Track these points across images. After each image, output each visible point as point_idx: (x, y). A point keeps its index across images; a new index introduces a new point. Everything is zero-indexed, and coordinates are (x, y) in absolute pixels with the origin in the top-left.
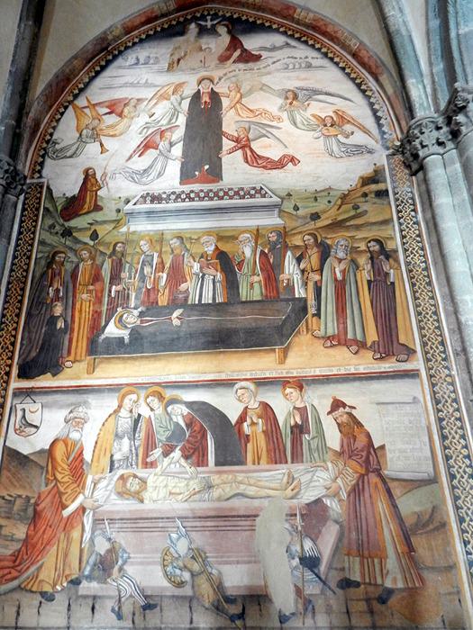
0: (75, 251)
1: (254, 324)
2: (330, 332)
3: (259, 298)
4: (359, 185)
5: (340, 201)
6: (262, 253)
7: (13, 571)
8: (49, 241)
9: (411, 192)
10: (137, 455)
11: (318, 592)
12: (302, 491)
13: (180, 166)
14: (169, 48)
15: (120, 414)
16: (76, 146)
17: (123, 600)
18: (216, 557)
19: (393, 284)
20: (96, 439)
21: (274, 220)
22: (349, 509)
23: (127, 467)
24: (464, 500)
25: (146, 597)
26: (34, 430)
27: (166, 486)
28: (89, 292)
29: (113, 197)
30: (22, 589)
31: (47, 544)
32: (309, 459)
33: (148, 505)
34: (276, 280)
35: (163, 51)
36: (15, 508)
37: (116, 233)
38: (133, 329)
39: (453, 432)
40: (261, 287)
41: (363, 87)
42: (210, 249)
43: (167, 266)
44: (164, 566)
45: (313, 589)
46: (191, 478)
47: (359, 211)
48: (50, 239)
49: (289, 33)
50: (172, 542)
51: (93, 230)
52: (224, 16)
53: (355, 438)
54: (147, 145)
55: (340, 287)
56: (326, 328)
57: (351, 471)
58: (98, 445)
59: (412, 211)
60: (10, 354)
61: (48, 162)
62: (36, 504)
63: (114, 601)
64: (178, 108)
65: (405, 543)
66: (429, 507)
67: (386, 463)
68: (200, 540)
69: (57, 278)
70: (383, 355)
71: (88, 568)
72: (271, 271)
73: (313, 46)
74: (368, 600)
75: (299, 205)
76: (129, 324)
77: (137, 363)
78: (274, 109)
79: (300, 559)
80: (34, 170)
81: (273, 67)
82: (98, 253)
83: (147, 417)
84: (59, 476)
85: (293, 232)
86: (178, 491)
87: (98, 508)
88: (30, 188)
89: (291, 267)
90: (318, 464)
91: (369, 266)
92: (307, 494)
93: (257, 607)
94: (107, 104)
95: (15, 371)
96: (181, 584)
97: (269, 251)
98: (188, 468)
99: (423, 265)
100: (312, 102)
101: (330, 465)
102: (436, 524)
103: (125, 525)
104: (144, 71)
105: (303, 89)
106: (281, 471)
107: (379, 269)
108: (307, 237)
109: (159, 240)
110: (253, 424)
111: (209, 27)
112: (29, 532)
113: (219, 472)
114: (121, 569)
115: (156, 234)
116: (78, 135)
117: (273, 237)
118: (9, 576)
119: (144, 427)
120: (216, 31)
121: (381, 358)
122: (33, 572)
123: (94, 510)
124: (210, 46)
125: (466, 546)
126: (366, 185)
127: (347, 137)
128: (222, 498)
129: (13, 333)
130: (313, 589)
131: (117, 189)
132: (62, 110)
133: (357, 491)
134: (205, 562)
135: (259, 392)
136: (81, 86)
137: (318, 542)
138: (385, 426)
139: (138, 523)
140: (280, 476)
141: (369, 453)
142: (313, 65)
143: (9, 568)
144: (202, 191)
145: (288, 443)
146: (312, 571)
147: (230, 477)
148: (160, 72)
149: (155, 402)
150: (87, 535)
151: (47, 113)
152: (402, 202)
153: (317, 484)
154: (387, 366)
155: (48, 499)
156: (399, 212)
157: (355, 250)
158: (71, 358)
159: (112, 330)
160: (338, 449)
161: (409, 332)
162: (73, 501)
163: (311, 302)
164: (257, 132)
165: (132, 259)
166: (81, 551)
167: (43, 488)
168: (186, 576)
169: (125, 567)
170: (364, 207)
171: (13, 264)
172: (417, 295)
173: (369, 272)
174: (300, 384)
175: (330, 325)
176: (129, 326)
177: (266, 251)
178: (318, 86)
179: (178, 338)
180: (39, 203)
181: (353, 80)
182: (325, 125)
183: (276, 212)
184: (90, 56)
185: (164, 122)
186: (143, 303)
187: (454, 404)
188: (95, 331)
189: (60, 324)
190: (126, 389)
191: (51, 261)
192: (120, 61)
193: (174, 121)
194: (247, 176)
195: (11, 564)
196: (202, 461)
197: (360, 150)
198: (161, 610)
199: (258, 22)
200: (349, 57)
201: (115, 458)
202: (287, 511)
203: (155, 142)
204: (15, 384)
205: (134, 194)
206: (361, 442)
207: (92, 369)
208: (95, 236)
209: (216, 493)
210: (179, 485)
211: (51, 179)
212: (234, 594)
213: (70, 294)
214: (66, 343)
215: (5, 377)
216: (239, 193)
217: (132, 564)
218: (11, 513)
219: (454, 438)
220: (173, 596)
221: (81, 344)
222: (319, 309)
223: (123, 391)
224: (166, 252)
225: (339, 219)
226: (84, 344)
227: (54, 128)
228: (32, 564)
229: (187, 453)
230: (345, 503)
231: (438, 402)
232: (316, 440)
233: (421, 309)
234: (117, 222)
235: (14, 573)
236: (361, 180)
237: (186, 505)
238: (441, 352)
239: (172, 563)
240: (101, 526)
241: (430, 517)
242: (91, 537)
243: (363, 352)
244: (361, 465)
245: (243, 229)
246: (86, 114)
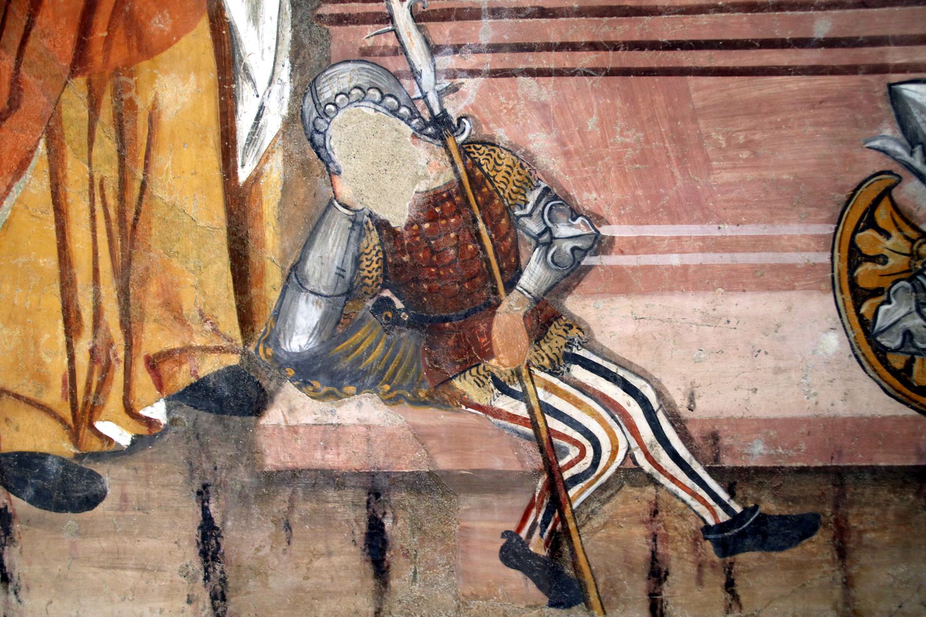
17: (577, 494)
25: (733, 479)
44: (859, 295)
63: (522, 502)
114: (544, 317)
150: (266, 98)
166: (238, 202)
169: (573, 305)
198: (842, 553)
217: (623, 283)
240: (368, 35)
242: (295, 118)
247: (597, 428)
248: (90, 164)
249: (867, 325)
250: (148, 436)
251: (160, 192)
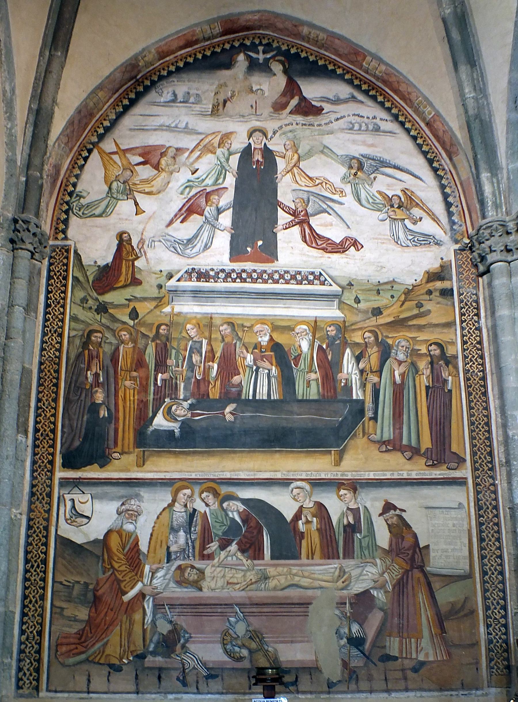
0: (113, 331)
1: (310, 425)
2: (386, 437)
3: (316, 397)
4: (424, 281)
5: (403, 296)
6: (320, 347)
7: (78, 646)
8: (81, 317)
9: (476, 294)
10: (194, 548)
11: (361, 664)
12: (352, 584)
13: (230, 238)
14: (213, 84)
15: (175, 509)
16: (105, 202)
17: (187, 671)
18: (273, 637)
19: (450, 391)
20: (151, 531)
21: (331, 312)
22: (393, 599)
23: (184, 558)
24: (492, 593)
26: (85, 520)
27: (224, 576)
28: (132, 379)
29: (153, 269)
30: (90, 662)
31: (110, 625)
32: (359, 556)
33: (206, 593)
34: (334, 380)
35: (206, 87)
36: (75, 592)
37: (158, 313)
38: (183, 422)
39: (490, 535)
40: (318, 385)
41: (435, 165)
42: (264, 340)
43: (218, 355)
44: (224, 644)
45: (357, 662)
46: (248, 570)
47: (422, 310)
49: (356, 82)
50: (230, 625)
51: (131, 307)
52: (279, 48)
53: (403, 538)
54: (190, 210)
55: (398, 391)
56: (382, 432)
57: (397, 567)
58: (154, 537)
59: (475, 315)
60: (51, 442)
61: (74, 220)
62: (95, 590)
64: (225, 164)
65: (439, 627)
66: (462, 597)
67: (429, 561)
68: (256, 623)
69: (95, 361)
70: (435, 462)
71: (152, 646)
73: (382, 104)
74: (403, 670)
75: (361, 297)
76: (179, 416)
77: (189, 458)
78: (336, 180)
79: (348, 639)
80: (57, 228)
81: (336, 125)
82: (140, 335)
83: (203, 512)
84: (116, 566)
85: (353, 327)
86: (235, 581)
87: (157, 594)
88: (55, 251)
89: (350, 366)
90: (368, 560)
91: (429, 371)
92: (356, 586)
93: (309, 677)
94: (140, 151)
95: (58, 460)
96: (241, 659)
97: (327, 346)
98: (244, 560)
99: (480, 374)
100: (380, 176)
101: (378, 561)
102: (466, 611)
103: (185, 610)
104: (183, 110)
105: (369, 158)
107: (438, 375)
108: (367, 335)
109: (207, 324)
110: (308, 522)
111: (261, 61)
112: (91, 614)
113: (276, 566)
115: (206, 318)
116: (106, 188)
117: (332, 331)
118: (76, 651)
119: (199, 522)
120: (269, 67)
121: (433, 466)
122: (99, 648)
123: (154, 596)
124: (262, 87)
125: (488, 628)
126: (431, 281)
127: (415, 223)
128: (278, 588)
129: (52, 419)
130: (357, 662)
131: (158, 260)
132: (85, 154)
134: (261, 641)
135: (314, 492)
136: (107, 123)
137: (364, 626)
138: (431, 528)
139: (200, 608)
140: (333, 570)
141: (414, 552)
142: (381, 128)
143: (74, 644)
144: (255, 271)
146: (358, 649)
147: (285, 570)
148: (203, 114)
149: (211, 499)
150: (149, 618)
151: (68, 156)
152: (467, 305)
153: (366, 577)
155: (107, 585)
156: (462, 315)
157: (414, 353)
158: (119, 449)
159: (160, 421)
160: (387, 548)
161: (461, 440)
162: (132, 588)
163: (369, 405)
164: (317, 206)
165: (179, 344)
166: (144, 631)
167: (101, 576)
168: (245, 652)
169: (187, 645)
170: (428, 306)
171: (43, 342)
172: (473, 404)
173: (428, 377)
174: (355, 486)
175: (386, 429)
176: (179, 419)
177: (324, 346)
178: (386, 157)
179: (233, 435)
180: (67, 271)
181: (425, 154)
182: (392, 206)
183: (336, 303)
184: (117, 86)
185: (209, 181)
186: (193, 395)
187: (494, 511)
188: (142, 422)
189: (103, 413)
190: (177, 485)
191: (86, 343)
192: (152, 96)
193: (220, 181)
194: (304, 258)
195: (76, 641)
196: (259, 555)
197: (427, 240)
199: (320, 63)
200: (423, 125)
201: (173, 548)
202: (337, 600)
203: (200, 207)
204: (60, 474)
205: (176, 268)
206: (408, 541)
207: (141, 463)
208: (134, 314)
209: (272, 583)
210: (236, 575)
211: (78, 241)
212: (289, 666)
213: (112, 380)
214: (112, 433)
215: (48, 466)
216: (296, 277)
217: (194, 642)
218: (70, 597)
219: (490, 540)
220: (233, 669)
222: (376, 413)
223: (177, 485)
224: (216, 339)
225: (401, 317)
226: (130, 436)
227: (77, 177)
228: (97, 641)
229: (243, 547)
230: (390, 594)
231: (480, 508)
232: (367, 539)
233: (474, 419)
234: (160, 301)
235: (81, 649)
236: (426, 275)
237: (243, 594)
238: (488, 462)
239: (231, 642)
240: (163, 610)
241: (462, 606)
242: (152, 620)
243: (416, 458)
244: (407, 563)
245: (300, 319)
246: (115, 163)
247: (190, 662)
248: (126, 626)
249: (225, 649)
250: (130, 662)
251: (134, 629)
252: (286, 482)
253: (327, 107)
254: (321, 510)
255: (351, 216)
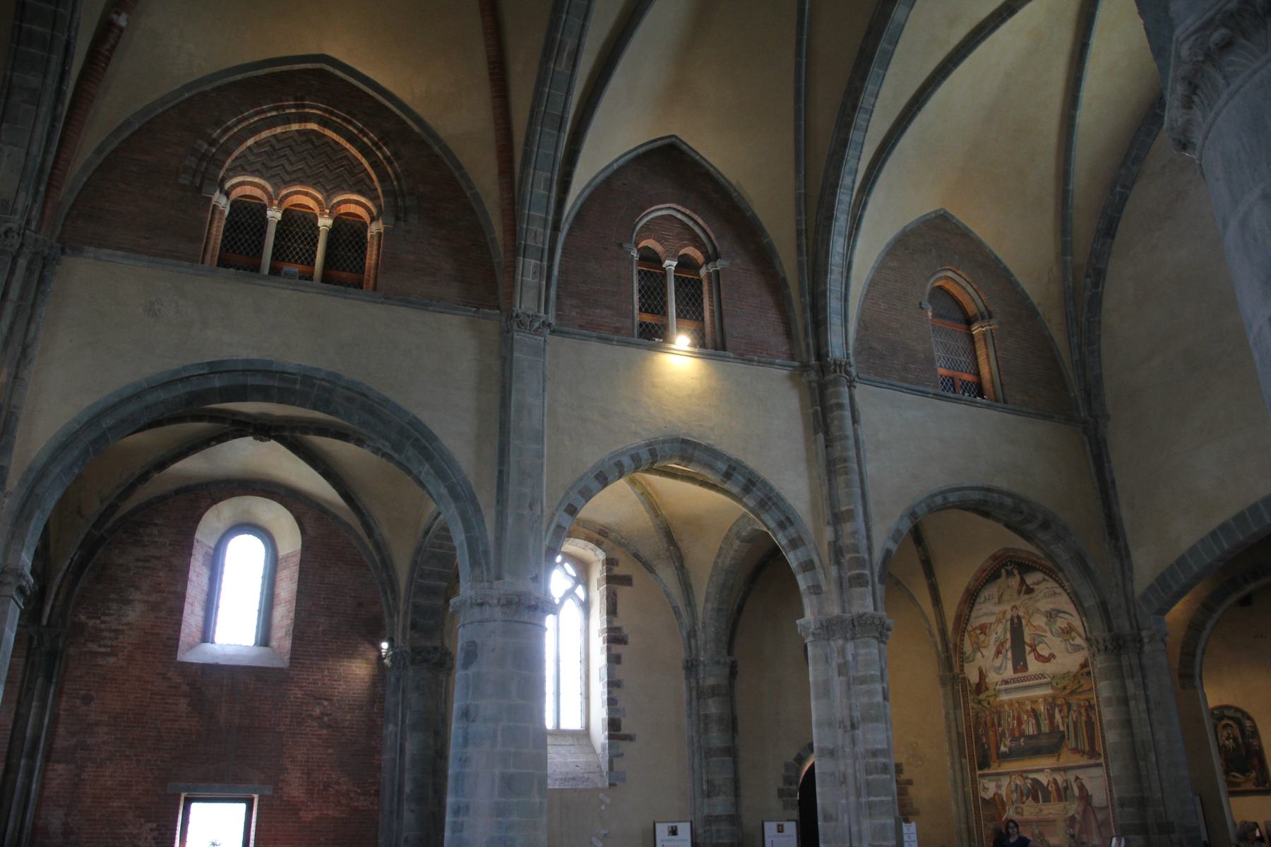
21: (1048, 691)
48: (975, 706)
55: (1075, 724)
72: (1051, 717)
78: (1043, 625)
106: (1062, 804)
109: (1011, 703)
131: (993, 677)
133: (1084, 811)
145: (1063, 794)
154: (1092, 762)
159: (1003, 749)
161: (1099, 748)
174: (1065, 769)
178: (1059, 607)
197: (1078, 648)
216: (1036, 677)
221: (994, 756)
234: (996, 696)
252: (1043, 769)
253: (1036, 587)
254: (1055, 781)
255: (1052, 643)
